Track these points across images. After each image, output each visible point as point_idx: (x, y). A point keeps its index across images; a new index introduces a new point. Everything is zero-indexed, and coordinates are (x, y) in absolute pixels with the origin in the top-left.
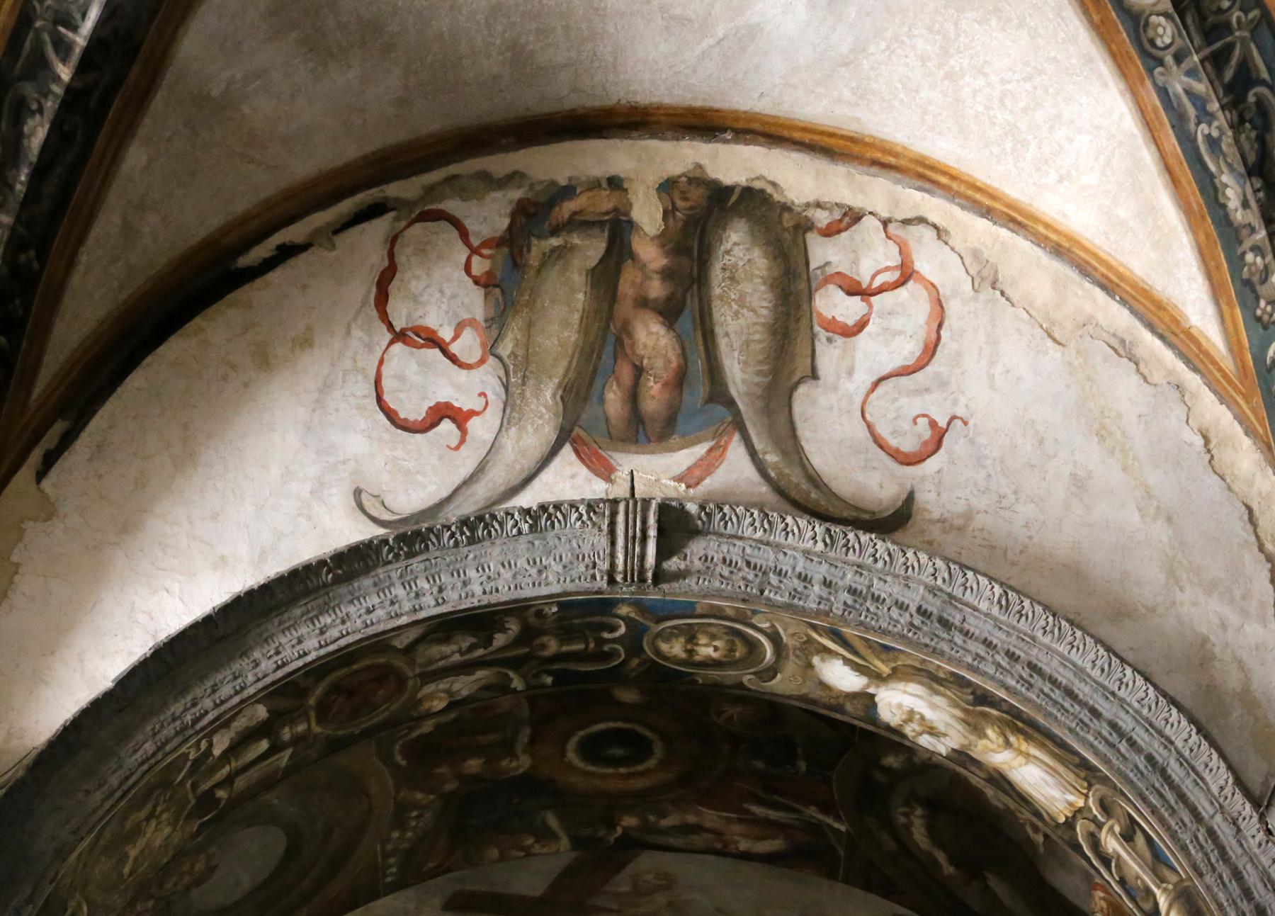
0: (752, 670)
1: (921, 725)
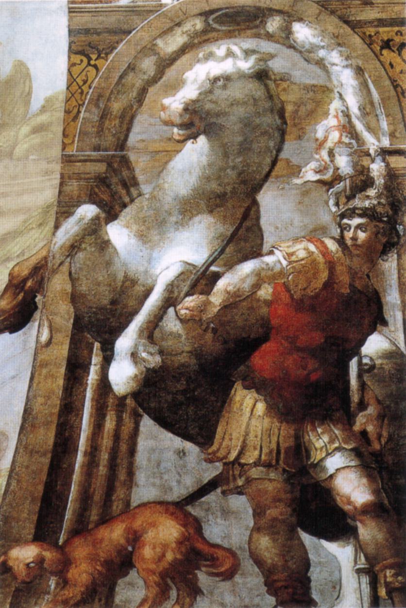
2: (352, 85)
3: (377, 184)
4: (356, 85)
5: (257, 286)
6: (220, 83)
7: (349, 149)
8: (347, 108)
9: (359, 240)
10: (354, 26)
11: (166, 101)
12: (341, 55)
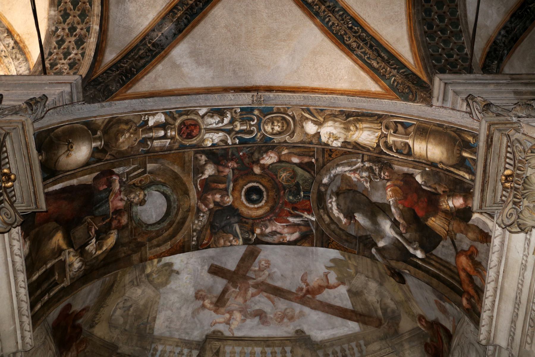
0: (288, 134)
1: (333, 137)
5: (399, 208)
10: (324, 165)
11: (344, 223)
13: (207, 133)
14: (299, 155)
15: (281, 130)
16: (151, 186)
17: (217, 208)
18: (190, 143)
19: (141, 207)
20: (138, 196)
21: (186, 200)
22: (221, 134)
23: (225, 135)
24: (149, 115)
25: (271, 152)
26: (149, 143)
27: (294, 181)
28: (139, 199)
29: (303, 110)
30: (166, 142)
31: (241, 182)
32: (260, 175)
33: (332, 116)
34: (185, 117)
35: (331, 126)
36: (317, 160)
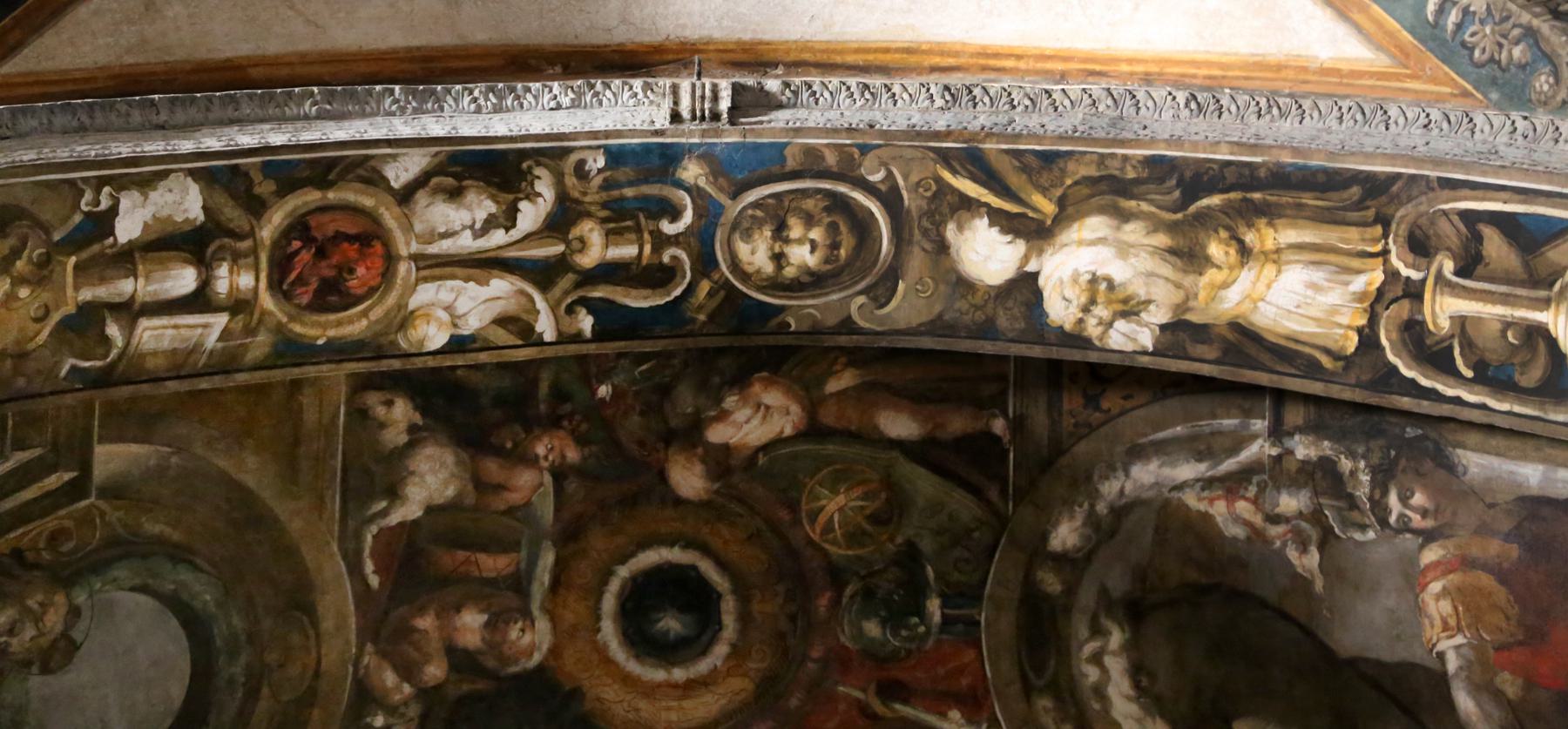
0: (859, 287)
1: (1109, 302)
2: (1160, 466)
3: (1330, 452)
4: (1158, 460)
6: (1145, 682)
7: (1268, 490)
8: (1198, 480)
9: (1426, 505)
12: (1107, 478)
13: (426, 280)
14: (913, 398)
15: (827, 261)
16: (108, 563)
17: (466, 687)
18: (332, 333)
19: (50, 679)
20: (38, 619)
21: (296, 639)
22: (502, 286)
23: (522, 292)
24: (121, 184)
25: (769, 383)
26: (113, 330)
27: (892, 539)
28: (41, 634)
29: (945, 157)
30: (205, 326)
31: (598, 542)
32: (703, 504)
33: (1103, 186)
34: (311, 197)
35: (1101, 241)
36: (1018, 425)
